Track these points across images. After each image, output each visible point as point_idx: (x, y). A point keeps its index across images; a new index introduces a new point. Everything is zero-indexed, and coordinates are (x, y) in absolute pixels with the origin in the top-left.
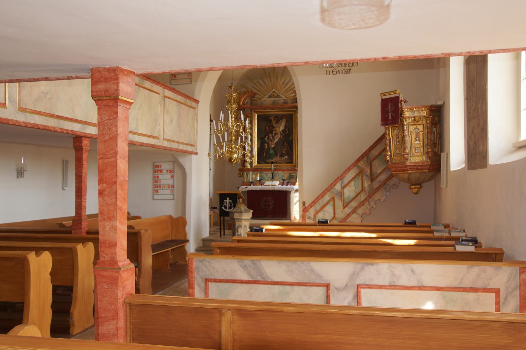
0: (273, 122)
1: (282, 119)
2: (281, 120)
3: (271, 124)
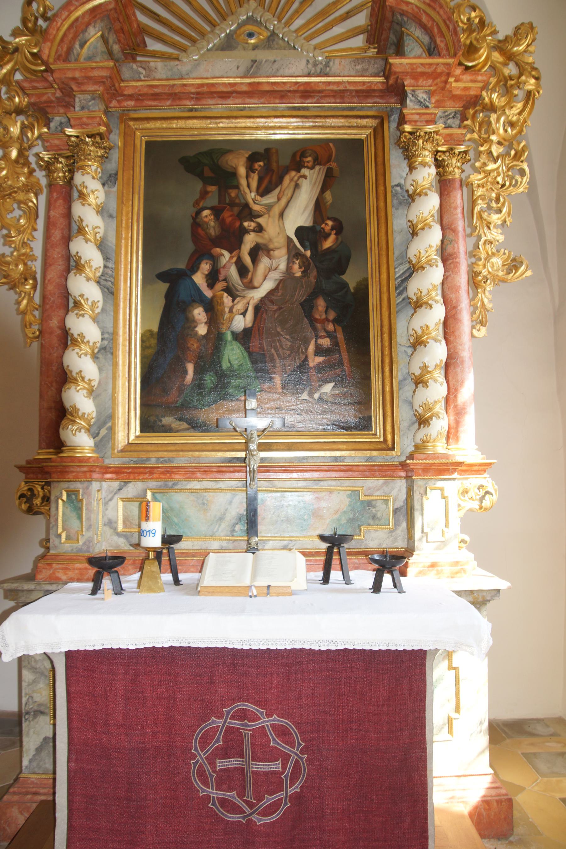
0: (243, 182)
2: (293, 173)
3: (233, 193)
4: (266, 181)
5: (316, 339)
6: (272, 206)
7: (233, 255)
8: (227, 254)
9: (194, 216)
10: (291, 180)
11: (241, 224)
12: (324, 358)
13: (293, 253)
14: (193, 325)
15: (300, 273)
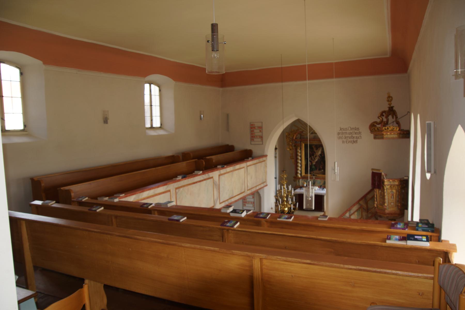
1: (320, 147)
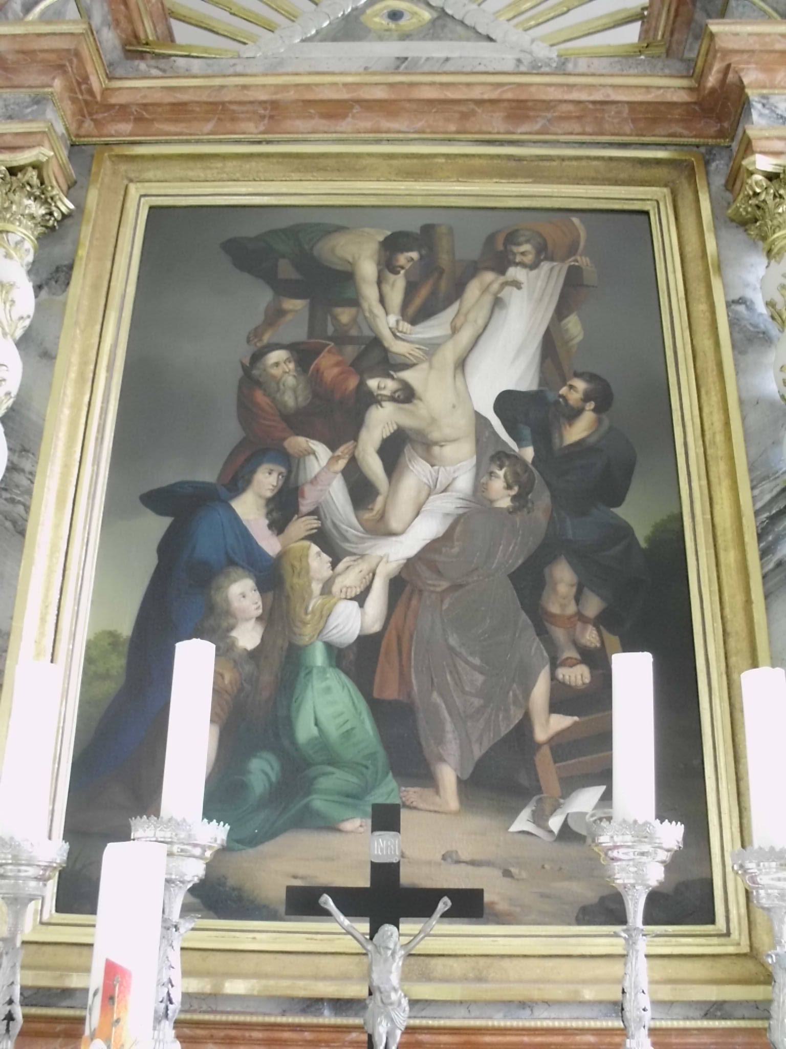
0: (370, 293)
2: (489, 276)
3: (345, 315)
4: (424, 292)
5: (554, 666)
6: (439, 345)
7: (339, 452)
8: (322, 451)
9: (247, 361)
10: (485, 290)
11: (362, 384)
12: (576, 718)
13: (491, 452)
14: (224, 625)
15: (509, 499)
